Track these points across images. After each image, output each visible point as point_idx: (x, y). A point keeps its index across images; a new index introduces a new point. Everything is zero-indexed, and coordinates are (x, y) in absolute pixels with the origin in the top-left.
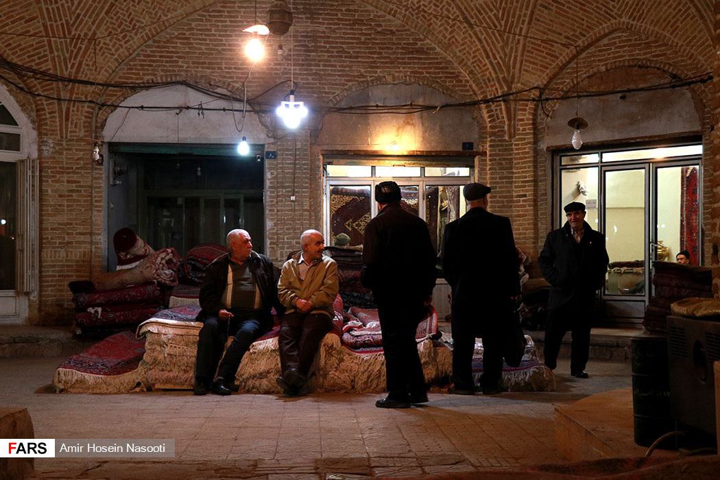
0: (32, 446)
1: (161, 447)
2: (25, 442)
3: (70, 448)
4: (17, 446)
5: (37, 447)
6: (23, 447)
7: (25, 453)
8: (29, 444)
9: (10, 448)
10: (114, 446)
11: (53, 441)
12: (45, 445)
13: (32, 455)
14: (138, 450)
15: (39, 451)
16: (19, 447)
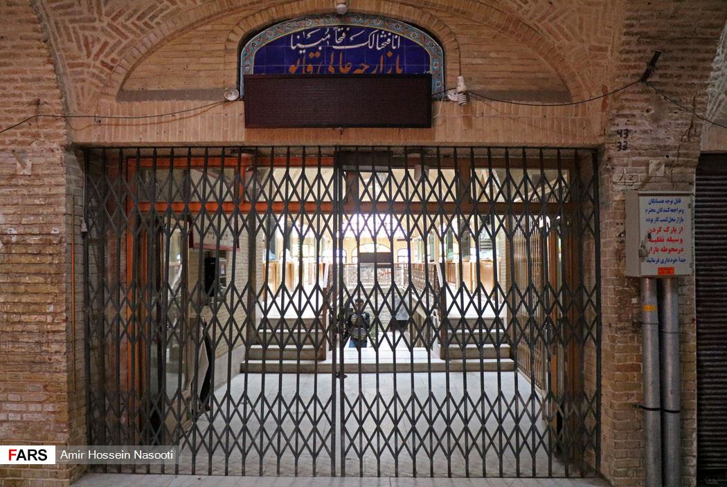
0: (32, 453)
1: (168, 453)
2: (25, 448)
3: (71, 455)
4: (17, 453)
5: (38, 453)
6: (23, 454)
7: (25, 459)
8: (29, 451)
9: (10, 455)
10: (121, 453)
11: (54, 447)
12: (45, 452)
13: (32, 461)
14: (145, 457)
15: (39, 458)
16: (20, 454)
